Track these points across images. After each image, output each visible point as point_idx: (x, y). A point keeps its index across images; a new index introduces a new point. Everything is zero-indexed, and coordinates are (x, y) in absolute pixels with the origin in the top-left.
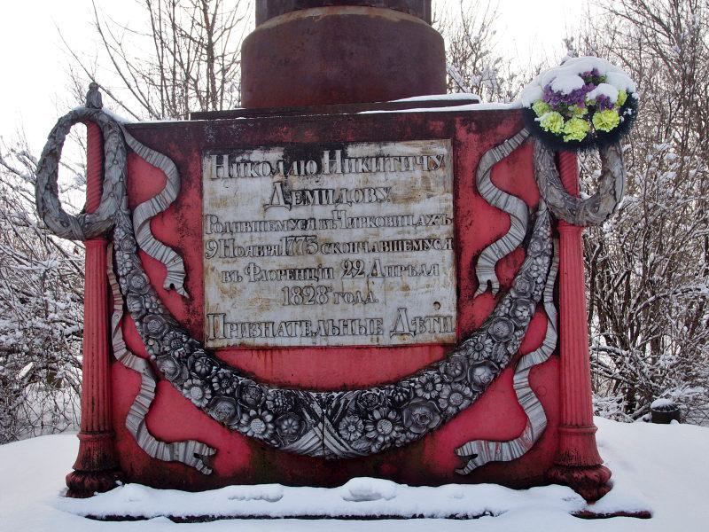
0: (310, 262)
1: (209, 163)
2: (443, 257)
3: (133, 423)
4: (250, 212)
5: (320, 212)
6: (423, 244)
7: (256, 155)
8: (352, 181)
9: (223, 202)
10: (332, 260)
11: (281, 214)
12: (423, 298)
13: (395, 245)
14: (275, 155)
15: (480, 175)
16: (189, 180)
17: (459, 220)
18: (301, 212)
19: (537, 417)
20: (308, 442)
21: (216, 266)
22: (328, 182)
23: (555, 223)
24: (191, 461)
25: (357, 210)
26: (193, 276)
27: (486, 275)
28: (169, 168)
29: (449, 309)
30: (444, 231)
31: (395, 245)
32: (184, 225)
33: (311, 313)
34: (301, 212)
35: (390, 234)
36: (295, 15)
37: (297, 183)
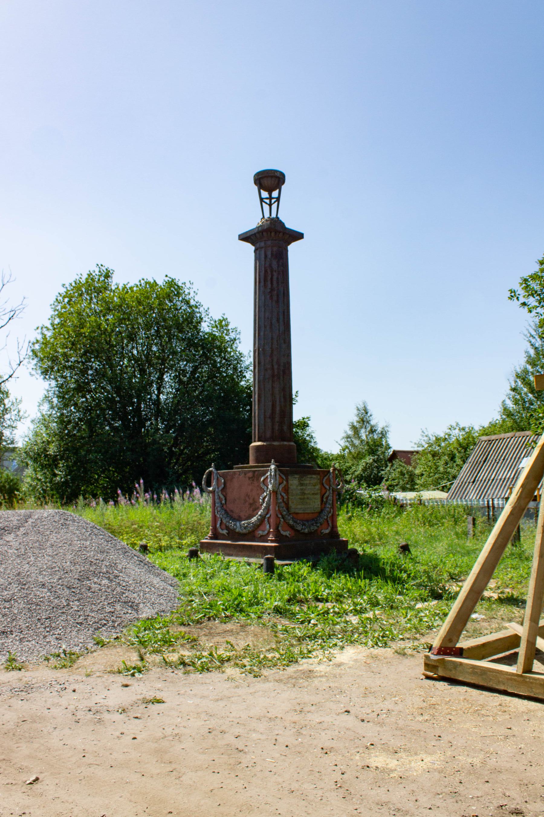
0: (303, 497)
1: (289, 477)
2: (318, 497)
3: (280, 528)
4: (295, 487)
5: (304, 487)
6: (316, 494)
7: (296, 476)
8: (308, 482)
9: (291, 485)
10: (306, 496)
11: (299, 488)
12: (315, 504)
13: (313, 494)
14: (298, 476)
15: (324, 482)
16: (287, 481)
17: (321, 489)
18: (302, 488)
19: (330, 524)
20: (306, 531)
21: (291, 497)
22: (305, 482)
23: (333, 490)
24: (288, 535)
25: (309, 487)
26: (288, 499)
27: (325, 500)
28: (284, 478)
29: (320, 506)
30: (319, 492)
31: (313, 494)
32: (286, 490)
33: (303, 506)
34: (302, 488)
35: (313, 492)
36: (282, 443)
37: (301, 482)
